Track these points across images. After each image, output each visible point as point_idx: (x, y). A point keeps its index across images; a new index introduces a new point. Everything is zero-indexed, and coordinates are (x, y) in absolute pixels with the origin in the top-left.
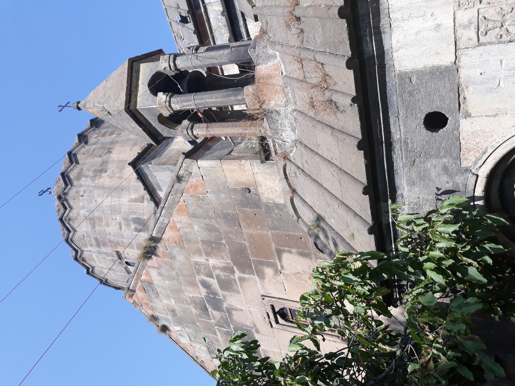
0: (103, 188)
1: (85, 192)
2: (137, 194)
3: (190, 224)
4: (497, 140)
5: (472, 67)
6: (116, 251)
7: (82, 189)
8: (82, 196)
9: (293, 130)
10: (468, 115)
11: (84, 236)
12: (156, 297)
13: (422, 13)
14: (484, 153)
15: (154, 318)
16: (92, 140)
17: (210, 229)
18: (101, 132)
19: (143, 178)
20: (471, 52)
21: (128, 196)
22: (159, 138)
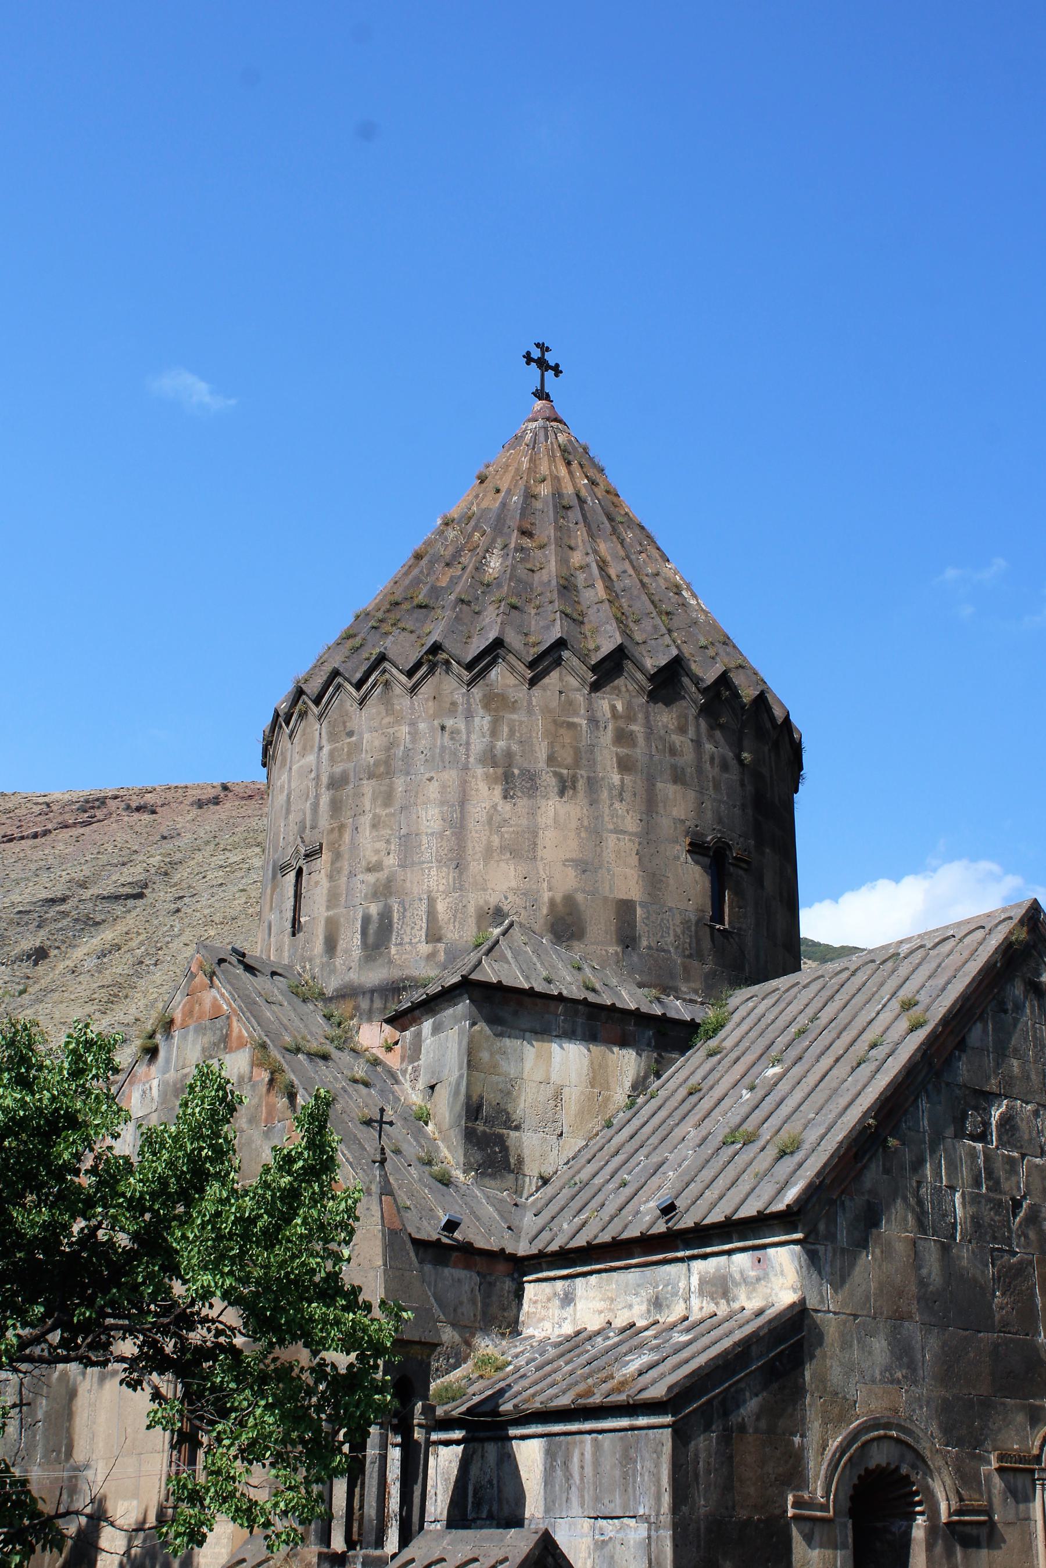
0: (463, 802)
1: (455, 732)
2: (446, 917)
6: (321, 845)
7: (462, 726)
8: (443, 728)
11: (350, 734)
12: (204, 1050)
15: (168, 1025)
16: (605, 703)
18: (630, 718)
21: (441, 888)
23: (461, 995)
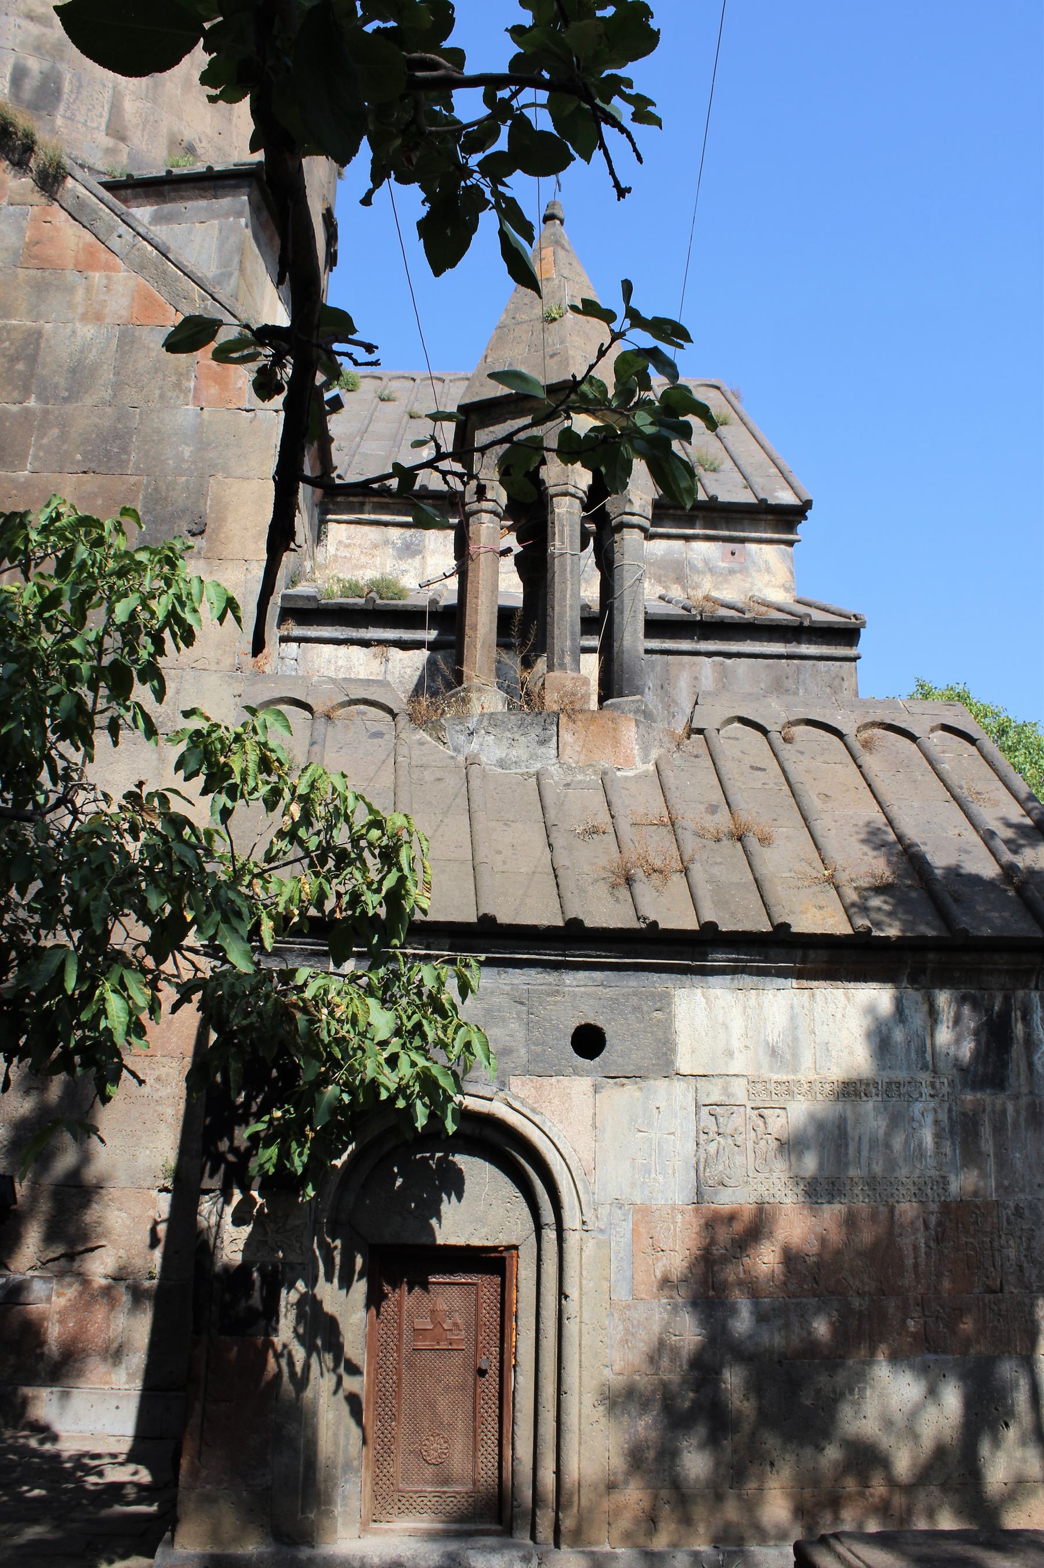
3: (98, 318)
4: (555, 1129)
5: (672, 1098)
9: (502, 764)
10: (596, 1089)
13: (750, 1034)
14: (533, 1110)
17: (80, 376)
19: (206, 184)
20: (691, 1095)
22: (474, 418)
23: (236, 187)
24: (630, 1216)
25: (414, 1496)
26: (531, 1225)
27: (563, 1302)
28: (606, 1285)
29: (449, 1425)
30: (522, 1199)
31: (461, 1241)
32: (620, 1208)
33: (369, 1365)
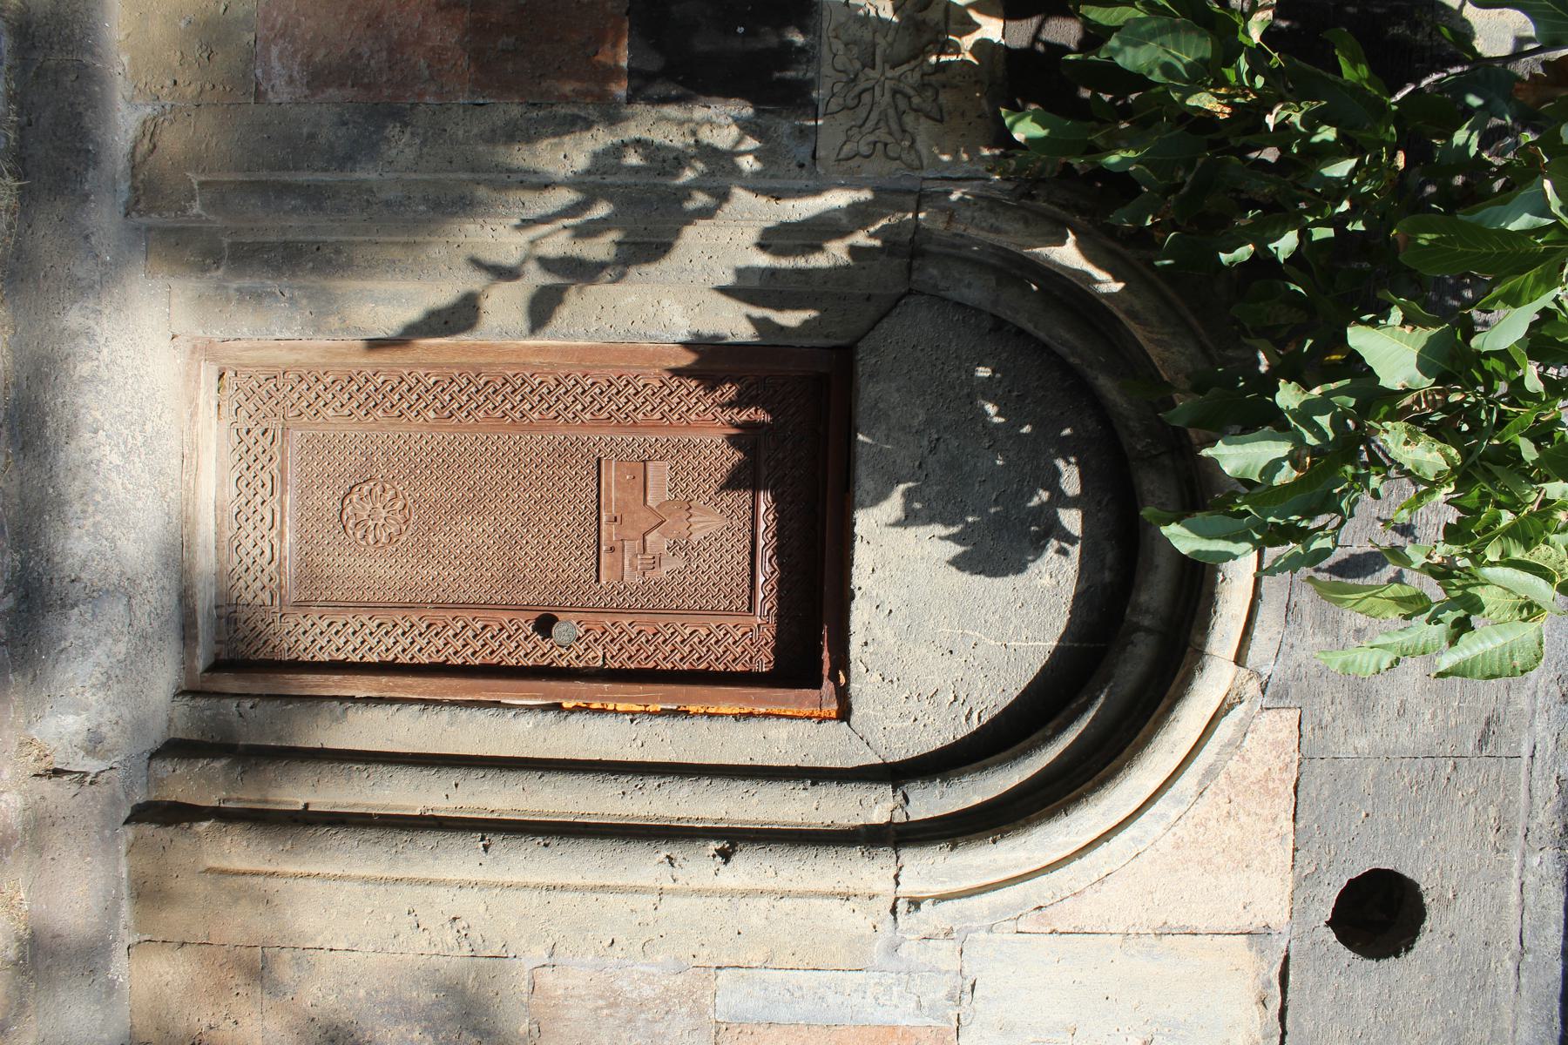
10: (1257, 936)
14: (1210, 773)
24: (929, 1021)
25: (274, 465)
26: (899, 752)
27: (714, 846)
28: (756, 957)
29: (429, 546)
30: (964, 731)
31: (861, 577)
32: (951, 997)
33: (564, 351)
